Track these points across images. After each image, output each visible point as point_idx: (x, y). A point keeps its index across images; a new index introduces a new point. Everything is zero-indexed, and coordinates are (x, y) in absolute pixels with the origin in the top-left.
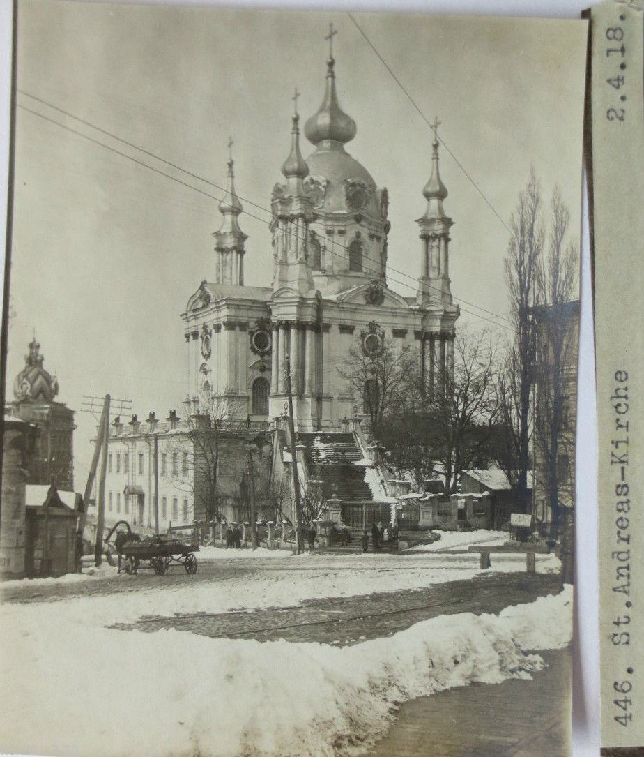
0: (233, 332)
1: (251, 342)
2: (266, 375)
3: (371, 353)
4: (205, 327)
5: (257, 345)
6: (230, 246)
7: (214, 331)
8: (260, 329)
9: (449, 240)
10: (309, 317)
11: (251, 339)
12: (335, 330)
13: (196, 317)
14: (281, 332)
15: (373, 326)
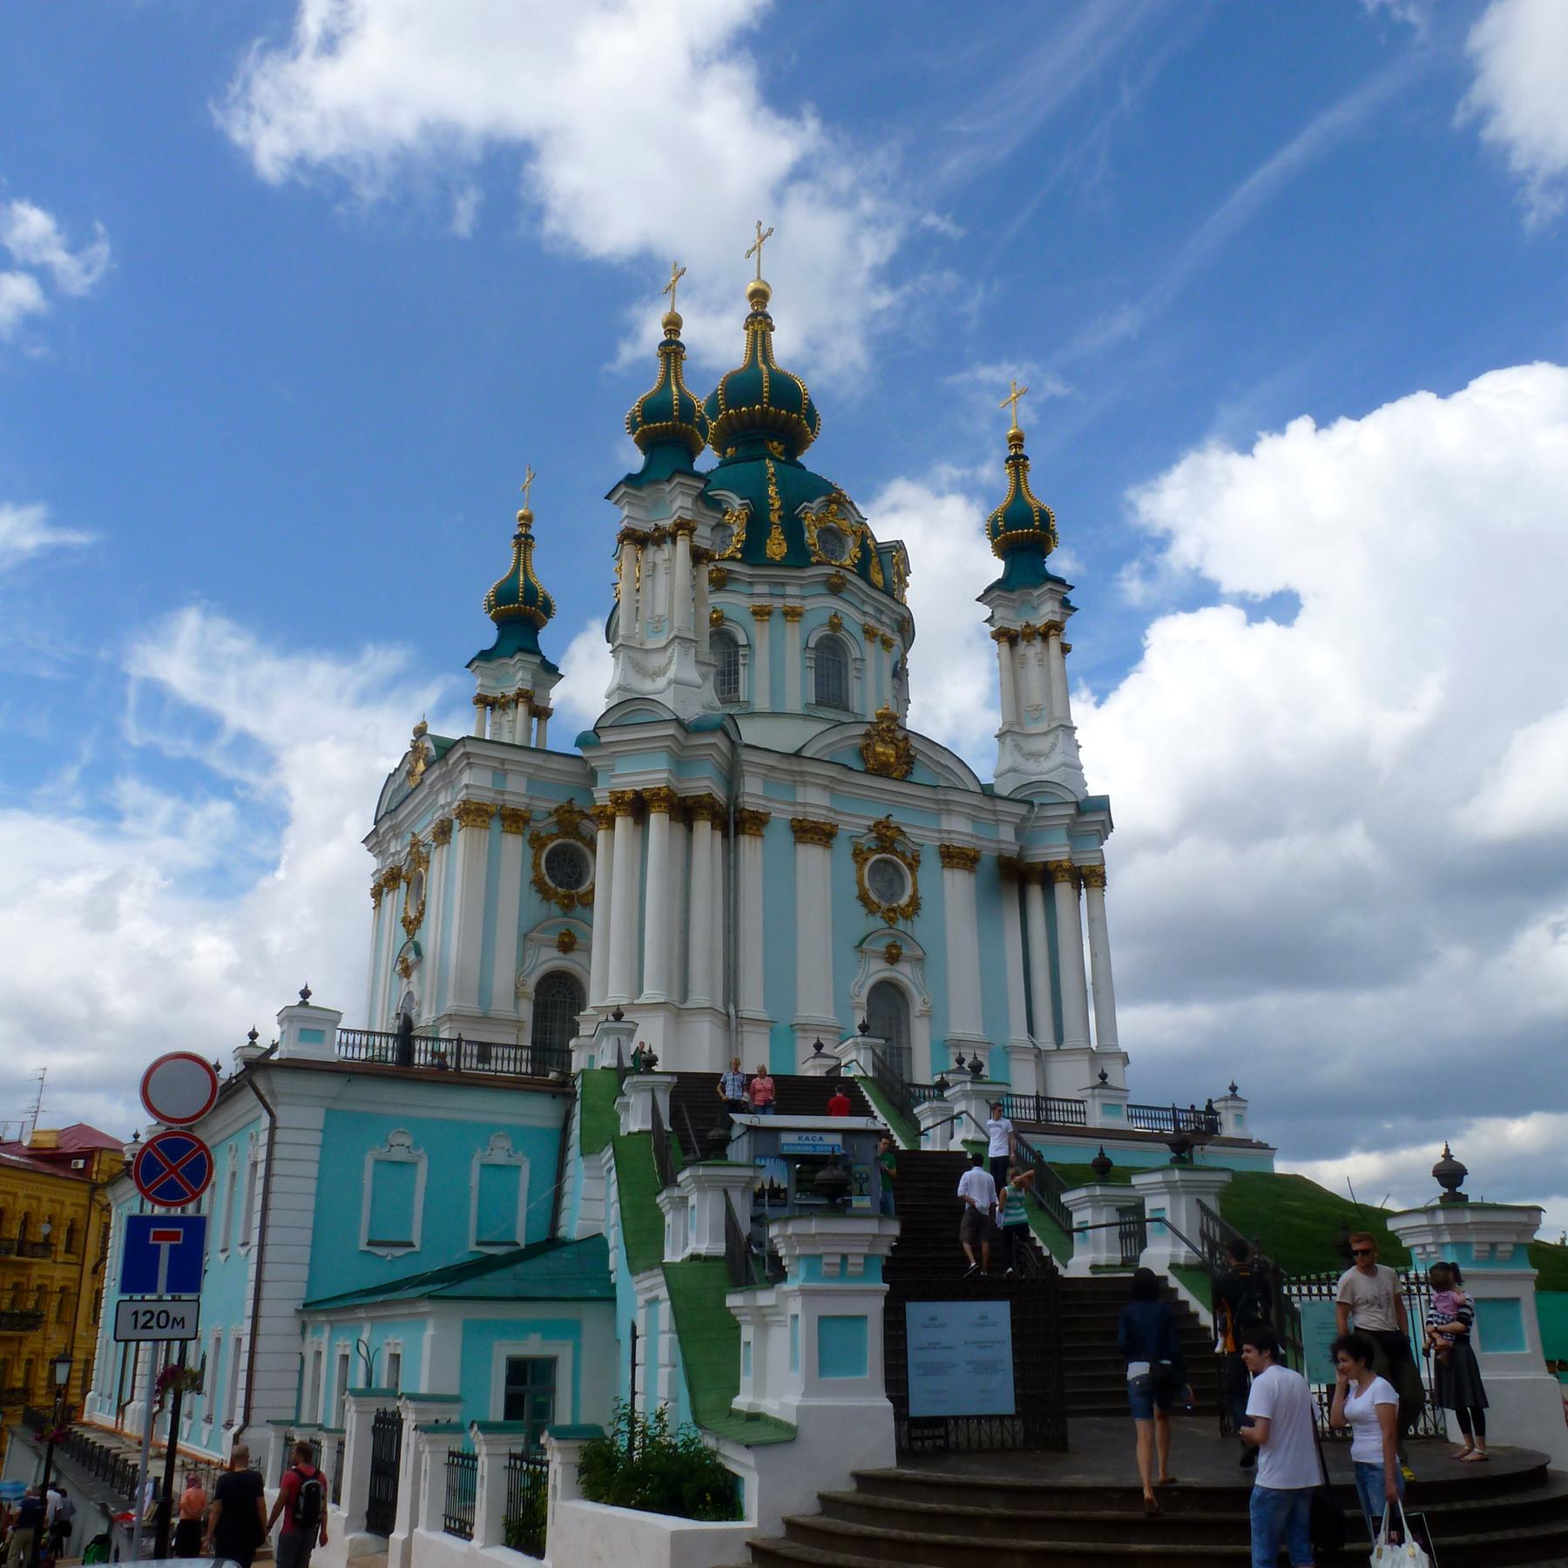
0: (484, 835)
1: (536, 866)
5: (553, 878)
6: (511, 692)
8: (566, 834)
10: (704, 783)
11: (537, 857)
12: (779, 833)
13: (396, 831)
15: (886, 836)
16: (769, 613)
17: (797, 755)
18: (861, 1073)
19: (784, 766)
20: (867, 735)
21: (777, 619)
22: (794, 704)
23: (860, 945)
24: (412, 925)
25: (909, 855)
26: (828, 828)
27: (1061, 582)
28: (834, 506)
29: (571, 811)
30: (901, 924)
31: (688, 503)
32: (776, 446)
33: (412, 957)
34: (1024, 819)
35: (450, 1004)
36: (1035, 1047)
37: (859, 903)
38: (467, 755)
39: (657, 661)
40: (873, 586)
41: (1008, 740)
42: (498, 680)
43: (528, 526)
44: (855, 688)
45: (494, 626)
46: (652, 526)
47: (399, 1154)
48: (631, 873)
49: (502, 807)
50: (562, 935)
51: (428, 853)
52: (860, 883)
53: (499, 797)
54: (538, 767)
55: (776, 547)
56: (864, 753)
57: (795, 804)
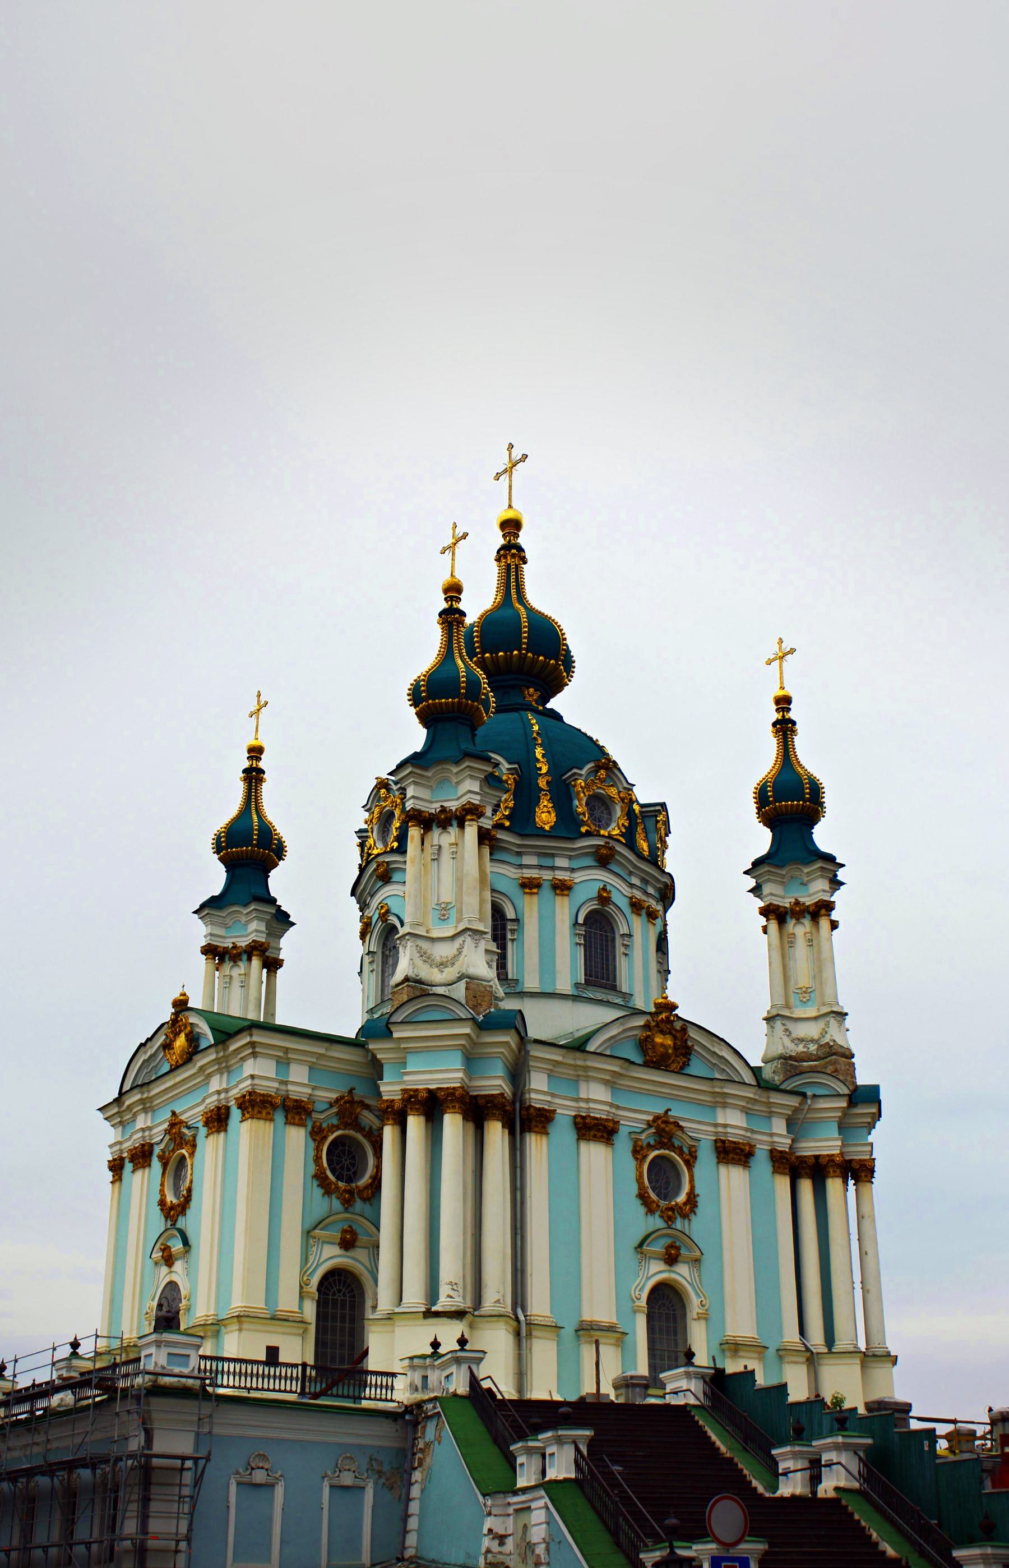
1: (317, 1159)
2: (354, 1261)
3: (663, 1203)
4: (175, 1123)
6: (243, 943)
7: (203, 1131)
8: (346, 1126)
9: (834, 925)
11: (318, 1149)
13: (147, 1106)
14: (415, 1124)
15: (665, 1130)
16: (539, 886)
17: (579, 1046)
18: (692, 1401)
19: (572, 1062)
20: (647, 1026)
21: (546, 891)
22: (564, 985)
23: (641, 1245)
24: (174, 1211)
25: (686, 1150)
26: (611, 1124)
27: (830, 859)
28: (602, 771)
29: (352, 1102)
30: (679, 1224)
31: (475, 786)
32: (532, 694)
33: (177, 1246)
34: (796, 1110)
35: (237, 1303)
36: (808, 1349)
37: (639, 1202)
38: (252, 1044)
39: (443, 951)
40: (640, 856)
41: (778, 1024)
42: (227, 927)
43: (259, 759)
44: (622, 965)
45: (222, 868)
46: (437, 805)
47: (259, 1477)
48: (424, 1176)
49: (286, 1098)
50: (344, 1232)
51: (194, 1137)
52: (639, 1179)
53: (283, 1087)
54: (320, 1056)
55: (545, 816)
56: (644, 1045)
57: (578, 1100)
